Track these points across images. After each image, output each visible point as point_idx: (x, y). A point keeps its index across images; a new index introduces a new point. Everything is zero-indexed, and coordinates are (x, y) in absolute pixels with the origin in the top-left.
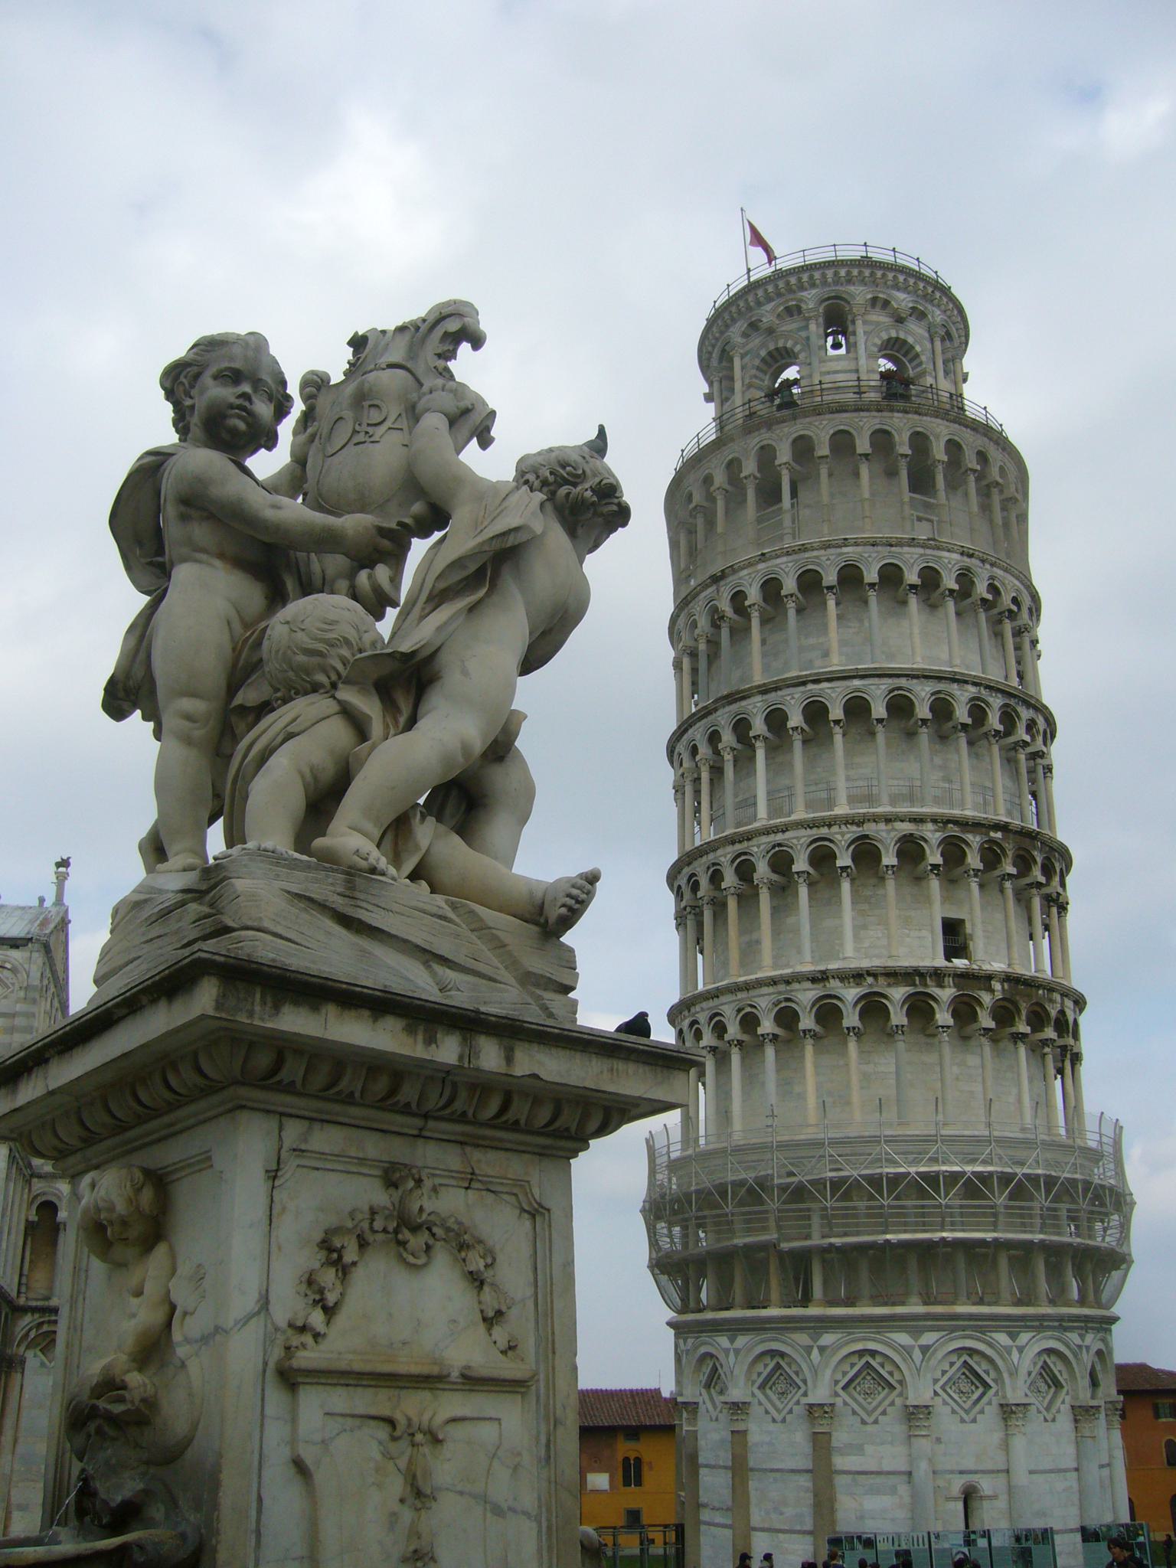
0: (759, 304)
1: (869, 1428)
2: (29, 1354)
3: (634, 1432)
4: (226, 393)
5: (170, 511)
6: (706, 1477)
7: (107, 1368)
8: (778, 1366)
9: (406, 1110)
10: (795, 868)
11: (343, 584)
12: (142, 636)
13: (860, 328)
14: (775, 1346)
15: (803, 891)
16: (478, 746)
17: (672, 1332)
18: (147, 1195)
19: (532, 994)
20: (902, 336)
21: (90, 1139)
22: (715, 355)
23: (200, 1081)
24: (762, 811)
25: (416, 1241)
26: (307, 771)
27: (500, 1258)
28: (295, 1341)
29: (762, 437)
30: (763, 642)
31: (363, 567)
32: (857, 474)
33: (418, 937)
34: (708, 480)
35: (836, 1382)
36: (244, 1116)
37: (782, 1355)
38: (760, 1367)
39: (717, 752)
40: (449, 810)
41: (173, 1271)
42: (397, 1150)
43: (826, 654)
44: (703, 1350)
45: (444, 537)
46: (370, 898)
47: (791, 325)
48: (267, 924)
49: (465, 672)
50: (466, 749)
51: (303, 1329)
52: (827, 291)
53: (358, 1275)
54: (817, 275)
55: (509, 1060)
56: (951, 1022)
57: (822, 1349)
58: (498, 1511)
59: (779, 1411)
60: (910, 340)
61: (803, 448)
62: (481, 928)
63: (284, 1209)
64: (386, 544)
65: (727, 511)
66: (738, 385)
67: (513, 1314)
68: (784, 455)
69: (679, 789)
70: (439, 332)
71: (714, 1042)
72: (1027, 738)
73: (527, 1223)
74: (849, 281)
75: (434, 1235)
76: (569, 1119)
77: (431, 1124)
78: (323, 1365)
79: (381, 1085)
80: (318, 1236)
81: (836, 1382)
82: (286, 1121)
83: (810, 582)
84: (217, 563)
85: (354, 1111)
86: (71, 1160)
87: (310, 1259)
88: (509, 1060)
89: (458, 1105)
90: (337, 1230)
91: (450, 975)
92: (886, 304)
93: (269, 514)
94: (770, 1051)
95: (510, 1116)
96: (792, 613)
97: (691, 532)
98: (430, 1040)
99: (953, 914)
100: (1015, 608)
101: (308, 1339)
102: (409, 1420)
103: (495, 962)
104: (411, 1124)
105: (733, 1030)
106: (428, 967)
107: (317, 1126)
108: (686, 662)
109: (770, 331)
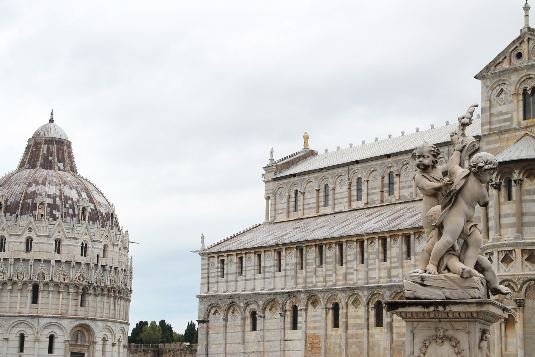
19: (465, 290)
26: (427, 250)
27: (461, 342)
33: (436, 285)
46: (426, 280)
49: (447, 226)
63: (416, 337)
73: (467, 335)
75: (443, 339)
77: (441, 320)
80: (422, 341)
84: (427, 197)
85: (425, 320)
87: (421, 345)
90: (425, 340)
91: (444, 290)
103: (455, 285)
104: (438, 320)
106: (441, 289)
107: (420, 323)
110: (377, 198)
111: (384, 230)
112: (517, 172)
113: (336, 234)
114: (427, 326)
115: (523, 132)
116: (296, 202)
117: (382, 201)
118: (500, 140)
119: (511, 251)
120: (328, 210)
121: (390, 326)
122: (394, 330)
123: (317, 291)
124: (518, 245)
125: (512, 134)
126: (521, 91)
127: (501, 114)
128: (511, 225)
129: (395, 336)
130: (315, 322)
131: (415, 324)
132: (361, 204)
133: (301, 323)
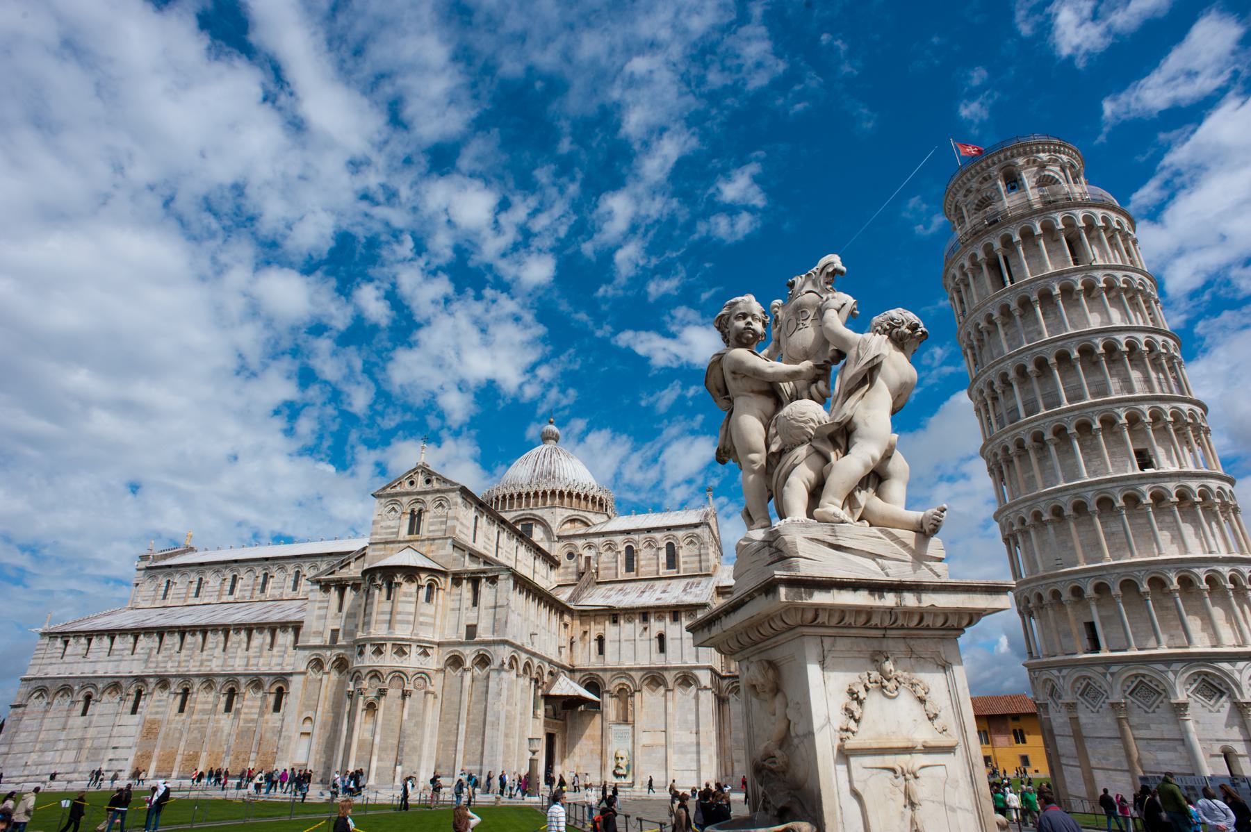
0: (969, 180)
1: (1147, 715)
2: (730, 696)
3: (1016, 717)
4: (741, 324)
5: (728, 377)
6: (1060, 741)
7: (766, 747)
8: (1088, 684)
9: (876, 627)
10: (1046, 438)
11: (805, 393)
12: (727, 430)
13: (1024, 175)
14: (1084, 673)
15: (1052, 449)
16: (878, 455)
17: (1026, 669)
18: (771, 674)
20: (1046, 173)
21: (743, 647)
22: (953, 209)
23: (785, 626)
24: (1022, 413)
25: (891, 685)
28: (844, 735)
29: (986, 240)
30: (1006, 334)
31: (813, 383)
32: (1038, 246)
34: (962, 267)
35: (1125, 691)
36: (806, 639)
37: (1090, 678)
38: (1078, 685)
39: (993, 391)
40: (871, 484)
41: (787, 706)
42: (875, 645)
43: (1040, 333)
44: (1044, 677)
45: (845, 364)
47: (986, 185)
48: (801, 554)
49: (866, 424)
50: (873, 460)
51: (847, 730)
52: (1002, 164)
53: (867, 703)
54: (995, 159)
55: (920, 601)
56: (1151, 501)
57: (1112, 674)
58: (953, 810)
59: (1094, 707)
60: (1052, 174)
61: (1007, 242)
62: (896, 539)
64: (821, 372)
65: (974, 277)
66: (967, 219)
67: (942, 714)
68: (997, 245)
69: (977, 410)
70: (824, 273)
71: (1020, 527)
72: (1164, 351)
74: (1012, 156)
76: (953, 622)
78: (858, 746)
79: (862, 619)
81: (1125, 691)
82: (824, 639)
83: (1026, 304)
84: (751, 394)
85: (853, 631)
86: (737, 656)
87: (845, 699)
88: (920, 601)
89: (899, 622)
92: (1035, 161)
93: (769, 370)
94: (1050, 528)
95: (924, 623)
96: (1018, 319)
97: (959, 292)
98: (881, 597)
99: (1140, 447)
100: (1141, 288)
101: (850, 734)
102: (902, 769)
105: (1028, 521)
106: (874, 560)
107: (838, 640)
108: (969, 351)
109: (978, 190)
110: (248, 594)
111: (253, 622)
112: (399, 576)
113: (203, 622)
114: (855, 648)
115: (406, 545)
116: (166, 591)
117: (252, 597)
118: (385, 549)
119: (382, 645)
120: (197, 601)
121: (238, 711)
122: (242, 716)
123: (169, 676)
124: (389, 639)
125: (397, 545)
126: (409, 511)
127: (389, 527)
128: (383, 622)
129: (241, 722)
130: (158, 706)
131: (827, 642)
132: (231, 599)
133: (142, 707)
